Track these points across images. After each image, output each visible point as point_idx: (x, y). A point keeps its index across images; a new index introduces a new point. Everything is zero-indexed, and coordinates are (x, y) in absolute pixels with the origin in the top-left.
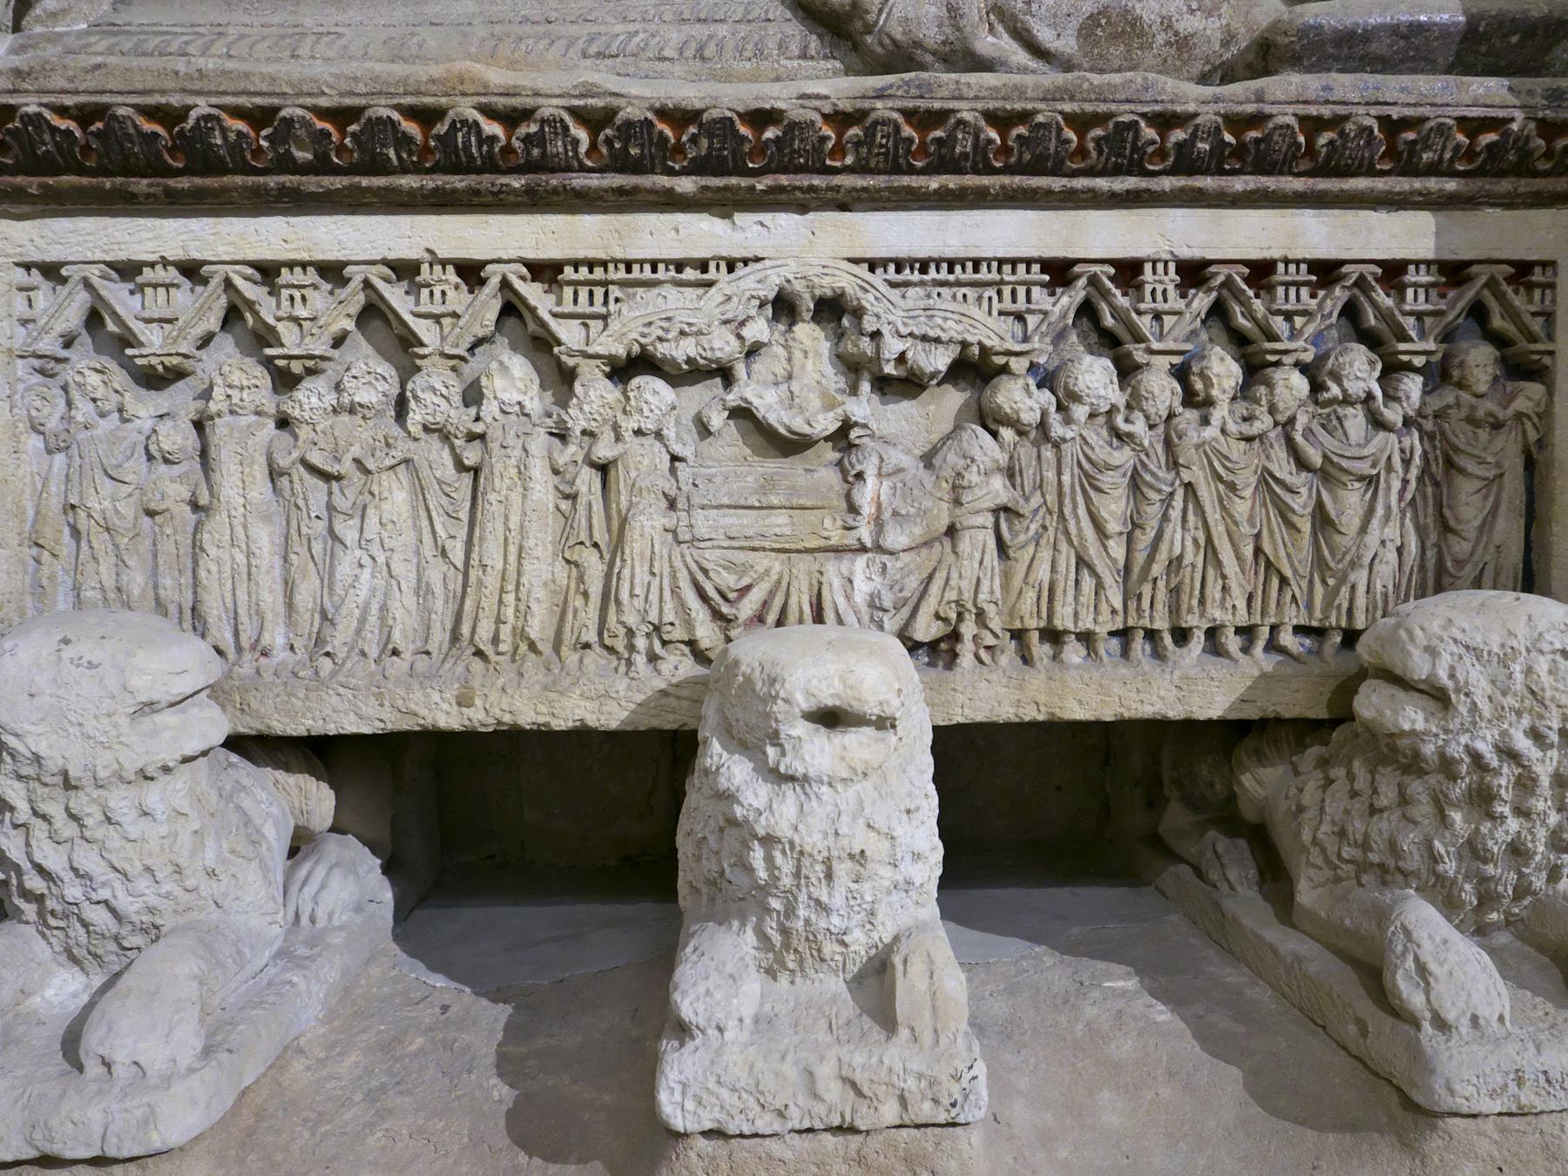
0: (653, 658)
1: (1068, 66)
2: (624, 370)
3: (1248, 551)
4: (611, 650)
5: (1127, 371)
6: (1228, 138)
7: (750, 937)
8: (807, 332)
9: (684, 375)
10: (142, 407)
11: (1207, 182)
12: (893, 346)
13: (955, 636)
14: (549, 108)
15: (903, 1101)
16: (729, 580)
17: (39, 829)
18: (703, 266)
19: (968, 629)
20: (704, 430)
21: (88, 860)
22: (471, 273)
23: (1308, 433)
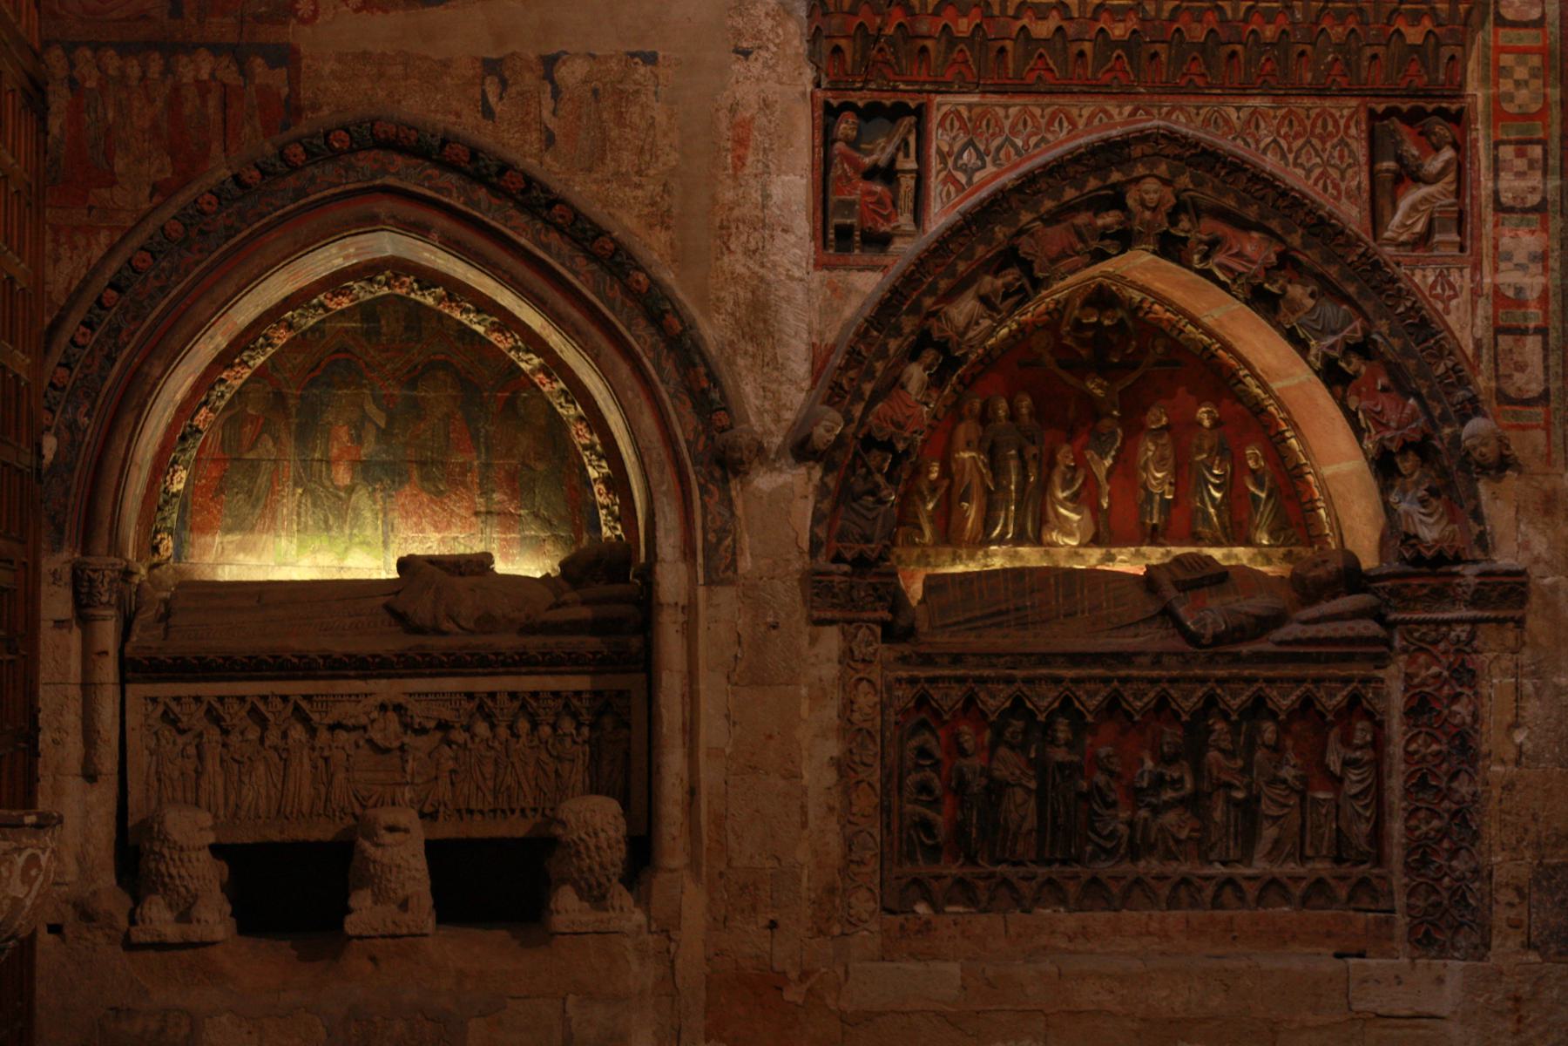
0: (341, 819)
1: (472, 632)
2: (332, 728)
3: (533, 783)
4: (328, 816)
5: (493, 727)
6: (517, 657)
7: (369, 892)
10: (181, 740)
11: (513, 669)
12: (417, 720)
13: (437, 812)
15: (408, 926)
17: (171, 863)
18: (357, 695)
19: (442, 809)
20: (357, 746)
21: (183, 872)
22: (285, 698)
23: (553, 745)
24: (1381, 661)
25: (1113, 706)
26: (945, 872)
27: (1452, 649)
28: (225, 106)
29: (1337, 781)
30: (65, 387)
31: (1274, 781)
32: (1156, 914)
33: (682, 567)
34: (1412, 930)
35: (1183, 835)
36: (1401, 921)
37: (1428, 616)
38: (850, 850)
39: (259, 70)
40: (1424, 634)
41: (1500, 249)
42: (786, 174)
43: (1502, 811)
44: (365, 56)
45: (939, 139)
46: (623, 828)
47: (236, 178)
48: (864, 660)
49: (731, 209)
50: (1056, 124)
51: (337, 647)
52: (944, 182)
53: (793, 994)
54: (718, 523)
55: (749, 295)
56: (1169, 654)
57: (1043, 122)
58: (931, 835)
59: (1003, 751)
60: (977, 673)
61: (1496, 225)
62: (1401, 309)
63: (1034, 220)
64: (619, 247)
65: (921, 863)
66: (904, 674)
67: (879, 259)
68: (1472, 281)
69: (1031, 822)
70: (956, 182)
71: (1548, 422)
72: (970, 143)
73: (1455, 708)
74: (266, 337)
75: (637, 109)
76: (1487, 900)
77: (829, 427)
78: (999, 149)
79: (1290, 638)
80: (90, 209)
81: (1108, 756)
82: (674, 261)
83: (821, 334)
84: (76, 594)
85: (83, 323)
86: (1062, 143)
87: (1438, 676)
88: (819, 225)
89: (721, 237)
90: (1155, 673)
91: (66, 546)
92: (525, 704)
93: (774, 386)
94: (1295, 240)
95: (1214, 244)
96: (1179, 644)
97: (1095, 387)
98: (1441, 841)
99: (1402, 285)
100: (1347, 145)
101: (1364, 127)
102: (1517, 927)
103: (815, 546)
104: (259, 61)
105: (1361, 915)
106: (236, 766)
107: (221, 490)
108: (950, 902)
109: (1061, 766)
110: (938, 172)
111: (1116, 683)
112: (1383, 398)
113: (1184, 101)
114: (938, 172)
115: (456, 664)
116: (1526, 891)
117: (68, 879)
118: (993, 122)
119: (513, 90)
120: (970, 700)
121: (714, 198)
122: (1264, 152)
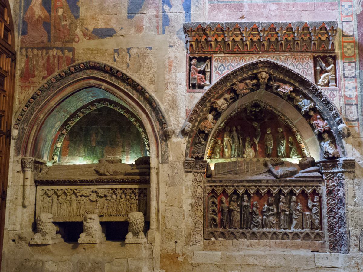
1: (112, 175)
2: (81, 196)
3: (125, 209)
5: (116, 196)
8: (94, 193)
9: (86, 197)
10: (48, 199)
12: (100, 194)
14: (76, 180)
16: (88, 211)
19: (105, 214)
20: (87, 200)
21: (45, 228)
22: (71, 189)
24: (320, 182)
25: (257, 192)
26: (218, 230)
27: (337, 179)
28: (59, 60)
29: (310, 210)
30: (21, 120)
31: (295, 210)
32: (268, 241)
33: (156, 159)
34: (330, 246)
35: (274, 222)
36: (327, 243)
37: (331, 171)
38: (196, 225)
39: (66, 53)
40: (331, 175)
41: (346, 86)
42: (181, 72)
43: (351, 217)
44: (89, 49)
45: (215, 64)
46: (143, 219)
47: (59, 75)
48: (199, 181)
49: (168, 80)
50: (241, 60)
51: (82, 178)
52: (216, 73)
53: (181, 259)
54: (164, 149)
55: (172, 99)
56: (270, 180)
57: (238, 60)
58: (215, 222)
59: (232, 202)
60: (225, 184)
61: (344, 81)
62: (323, 100)
63: (236, 81)
64: (142, 88)
65: (213, 228)
66: (209, 185)
67: (201, 90)
68: (339, 93)
69: (239, 219)
70: (219, 73)
71: (359, 125)
72: (222, 65)
73: (339, 192)
74: (78, 115)
75: (148, 59)
76: (349, 239)
77: (189, 126)
78: (228, 66)
79: (298, 176)
80: (29, 82)
81: (256, 204)
82: (155, 91)
83: (188, 107)
84: (22, 165)
85: (25, 106)
86: (242, 64)
87: (334, 185)
88: (188, 83)
89: (166, 86)
90: (267, 185)
91: (20, 154)
92: (124, 191)
93: (177, 119)
94: (297, 85)
95: (278, 87)
96: (273, 178)
97: (255, 124)
98: (336, 224)
99: (322, 94)
100: (309, 64)
101: (312, 60)
102: (357, 246)
103: (187, 155)
104: (66, 51)
105: (317, 242)
106: (60, 205)
107: (68, 147)
108: (220, 237)
109: (245, 206)
110: (215, 71)
111: (258, 187)
112: (318, 120)
113: (271, 55)
114: (215, 71)
115: (108, 182)
116: (358, 237)
117: (17, 229)
118: (227, 60)
119: (120, 56)
120: (224, 191)
121: (164, 78)
122: (289, 65)
